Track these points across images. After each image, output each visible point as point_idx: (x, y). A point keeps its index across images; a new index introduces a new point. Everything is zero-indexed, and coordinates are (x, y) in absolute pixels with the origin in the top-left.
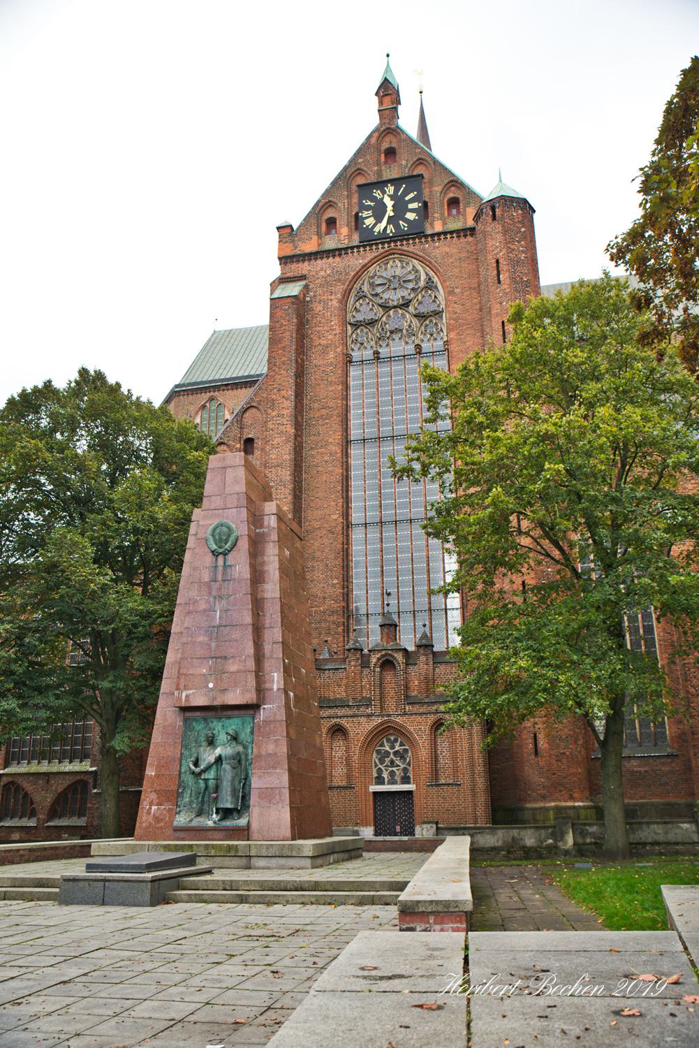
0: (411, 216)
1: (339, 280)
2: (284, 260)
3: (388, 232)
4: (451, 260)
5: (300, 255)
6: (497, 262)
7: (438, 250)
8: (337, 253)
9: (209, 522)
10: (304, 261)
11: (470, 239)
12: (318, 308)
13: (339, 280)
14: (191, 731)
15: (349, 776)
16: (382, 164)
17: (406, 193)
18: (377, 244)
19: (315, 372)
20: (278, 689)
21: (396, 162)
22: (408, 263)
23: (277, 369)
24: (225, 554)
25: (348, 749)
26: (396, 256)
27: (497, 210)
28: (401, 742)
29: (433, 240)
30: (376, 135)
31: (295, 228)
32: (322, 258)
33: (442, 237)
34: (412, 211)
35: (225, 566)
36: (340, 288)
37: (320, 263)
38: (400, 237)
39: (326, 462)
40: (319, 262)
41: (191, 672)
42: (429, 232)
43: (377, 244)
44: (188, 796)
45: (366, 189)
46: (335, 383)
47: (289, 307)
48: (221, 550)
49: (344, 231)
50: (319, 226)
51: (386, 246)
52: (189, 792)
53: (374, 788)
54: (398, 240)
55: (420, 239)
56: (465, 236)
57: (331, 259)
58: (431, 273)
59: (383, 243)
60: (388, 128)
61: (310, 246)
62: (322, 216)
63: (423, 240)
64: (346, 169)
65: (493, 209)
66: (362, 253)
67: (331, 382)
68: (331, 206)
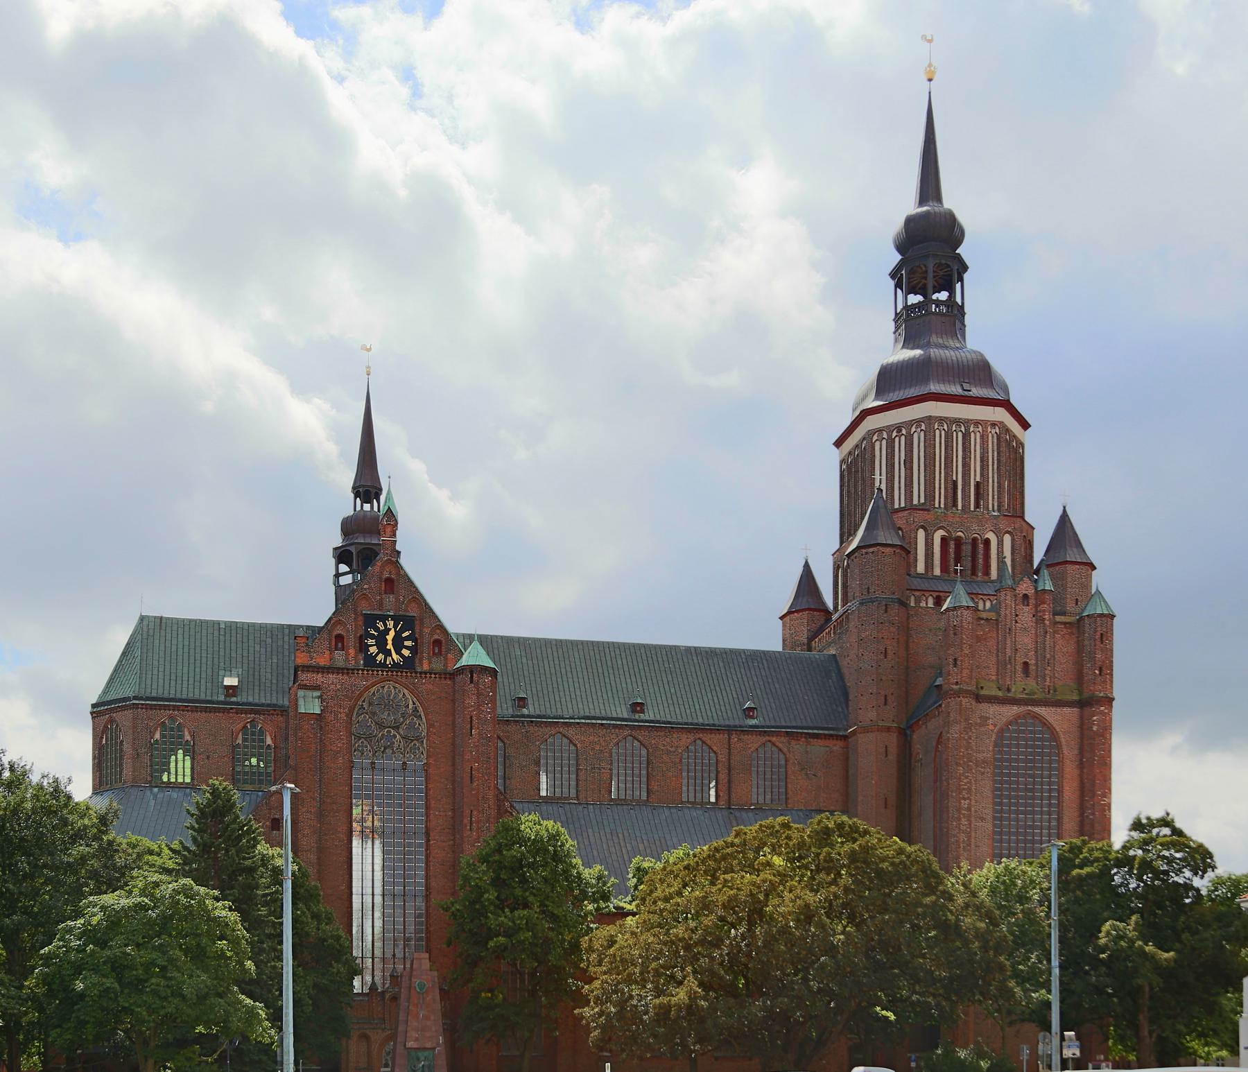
1: (346, 696)
7: (425, 685)
34: (407, 648)
36: (347, 703)
49: (352, 652)
61: (323, 662)
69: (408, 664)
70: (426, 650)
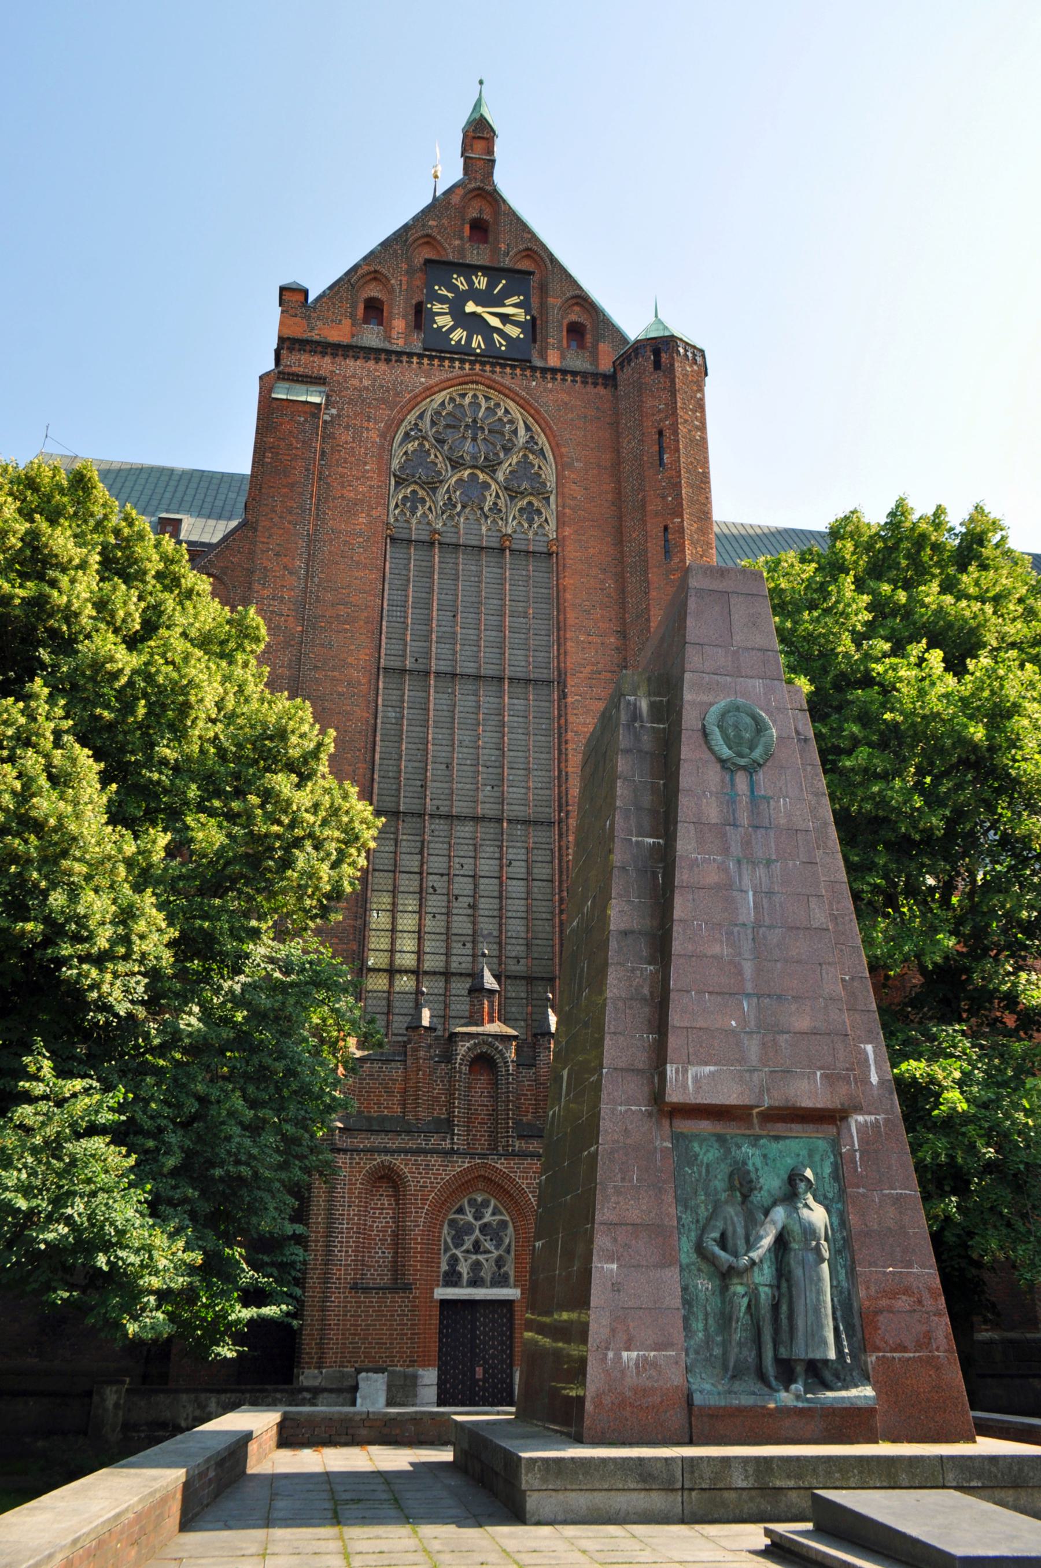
0: (513, 331)
1: (383, 401)
2: (286, 344)
3: (474, 345)
4: (570, 416)
5: (318, 343)
6: (660, 433)
7: (551, 395)
8: (383, 356)
9: (710, 698)
10: (324, 354)
11: (601, 390)
12: (346, 437)
13: (383, 401)
14: (690, 1165)
15: (397, 1268)
16: (466, 239)
17: (506, 293)
18: (452, 360)
19: (331, 540)
20: (882, 1082)
21: (485, 241)
22: (498, 405)
23: (276, 519)
24: (752, 769)
25: (400, 1215)
26: (481, 387)
27: (663, 355)
28: (495, 1207)
29: (544, 378)
30: (460, 192)
31: (311, 298)
32: (356, 358)
33: (559, 376)
35: (755, 800)
36: (385, 413)
37: (352, 366)
38: (491, 358)
39: (339, 694)
40: (350, 362)
41: (701, 1023)
42: (538, 363)
43: (452, 360)
44: (701, 1326)
45: (439, 269)
46: (365, 566)
47: (306, 420)
48: (742, 762)
49: (399, 325)
50: (354, 306)
51: (467, 366)
52: (701, 1316)
53: (443, 1293)
54: (488, 362)
55: (523, 369)
56: (595, 384)
57: (371, 364)
58: (536, 427)
59: (462, 361)
60: (479, 188)
61: (338, 334)
62: (364, 288)
63: (528, 373)
64: (406, 228)
65: (657, 353)
66: (426, 367)
67: (358, 563)
68: (375, 279)
69: (517, 359)
70: (555, 336)
